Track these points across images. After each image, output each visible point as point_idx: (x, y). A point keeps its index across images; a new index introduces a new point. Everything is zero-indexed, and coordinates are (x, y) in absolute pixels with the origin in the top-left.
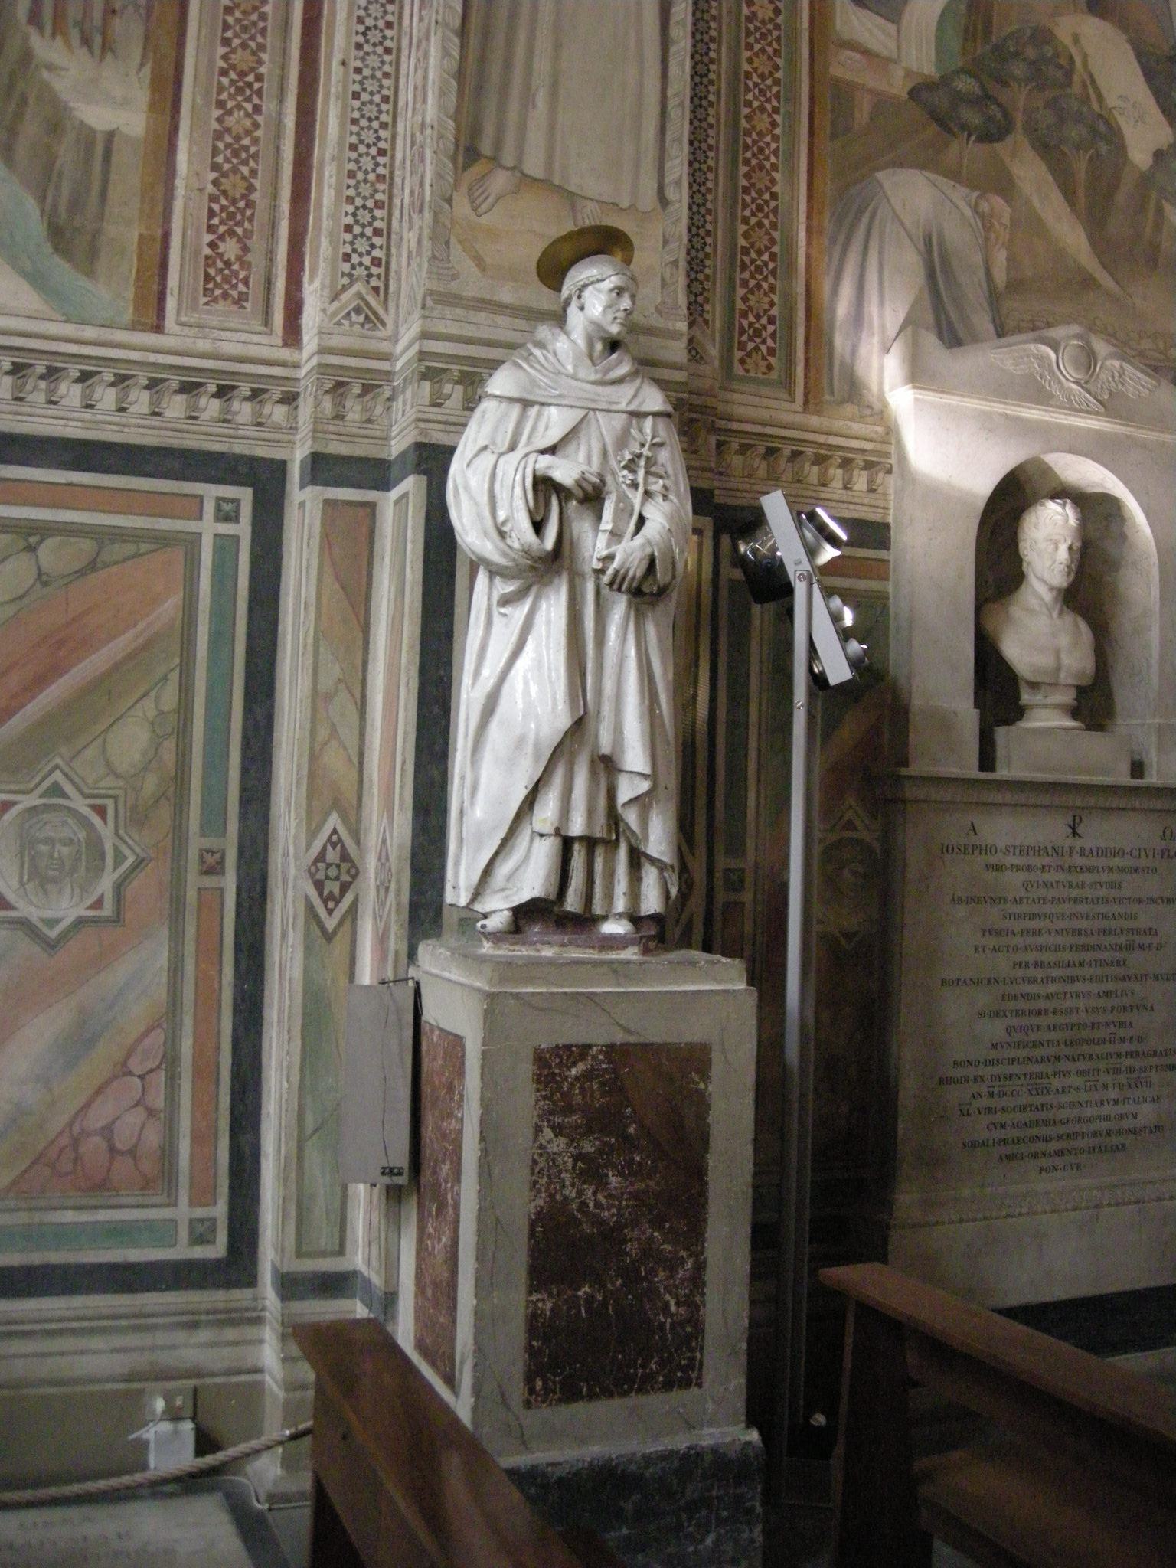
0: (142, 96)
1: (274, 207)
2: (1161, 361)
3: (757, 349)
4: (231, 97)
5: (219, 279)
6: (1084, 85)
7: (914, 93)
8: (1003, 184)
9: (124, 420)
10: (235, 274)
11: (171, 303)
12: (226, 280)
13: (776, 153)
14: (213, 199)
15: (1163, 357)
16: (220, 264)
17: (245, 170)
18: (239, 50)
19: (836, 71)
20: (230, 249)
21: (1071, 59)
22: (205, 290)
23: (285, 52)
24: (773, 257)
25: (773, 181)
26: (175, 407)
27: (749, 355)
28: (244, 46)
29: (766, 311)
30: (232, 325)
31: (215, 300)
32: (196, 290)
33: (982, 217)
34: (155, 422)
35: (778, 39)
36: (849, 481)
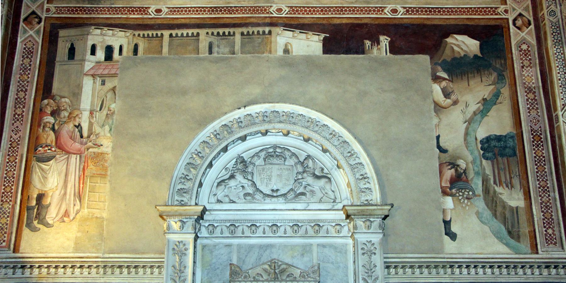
0: (521, 195)
1: (558, 219)
4: (542, 194)
5: (549, 239)
9: (534, 277)
10: (553, 237)
11: (539, 247)
12: (551, 239)
14: (544, 219)
16: (548, 235)
17: (549, 211)
18: (542, 182)
20: (550, 231)
22: (546, 242)
23: (552, 180)
26: (545, 272)
28: (543, 180)
30: (554, 250)
31: (549, 244)
32: (544, 243)
34: (541, 276)
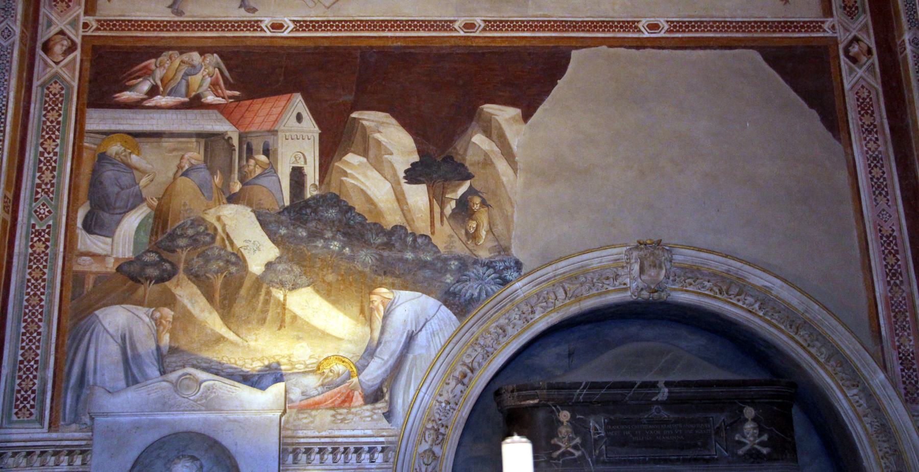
2: (266, 371)
3: (25, 407)
6: (223, 240)
7: (119, 269)
8: (170, 301)
13: (41, 314)
15: (267, 369)
19: (76, 268)
21: (215, 229)
24: (36, 362)
25: (39, 327)
27: (20, 410)
29: (30, 388)
33: (156, 320)
35: (46, 261)
36: (72, 461)
